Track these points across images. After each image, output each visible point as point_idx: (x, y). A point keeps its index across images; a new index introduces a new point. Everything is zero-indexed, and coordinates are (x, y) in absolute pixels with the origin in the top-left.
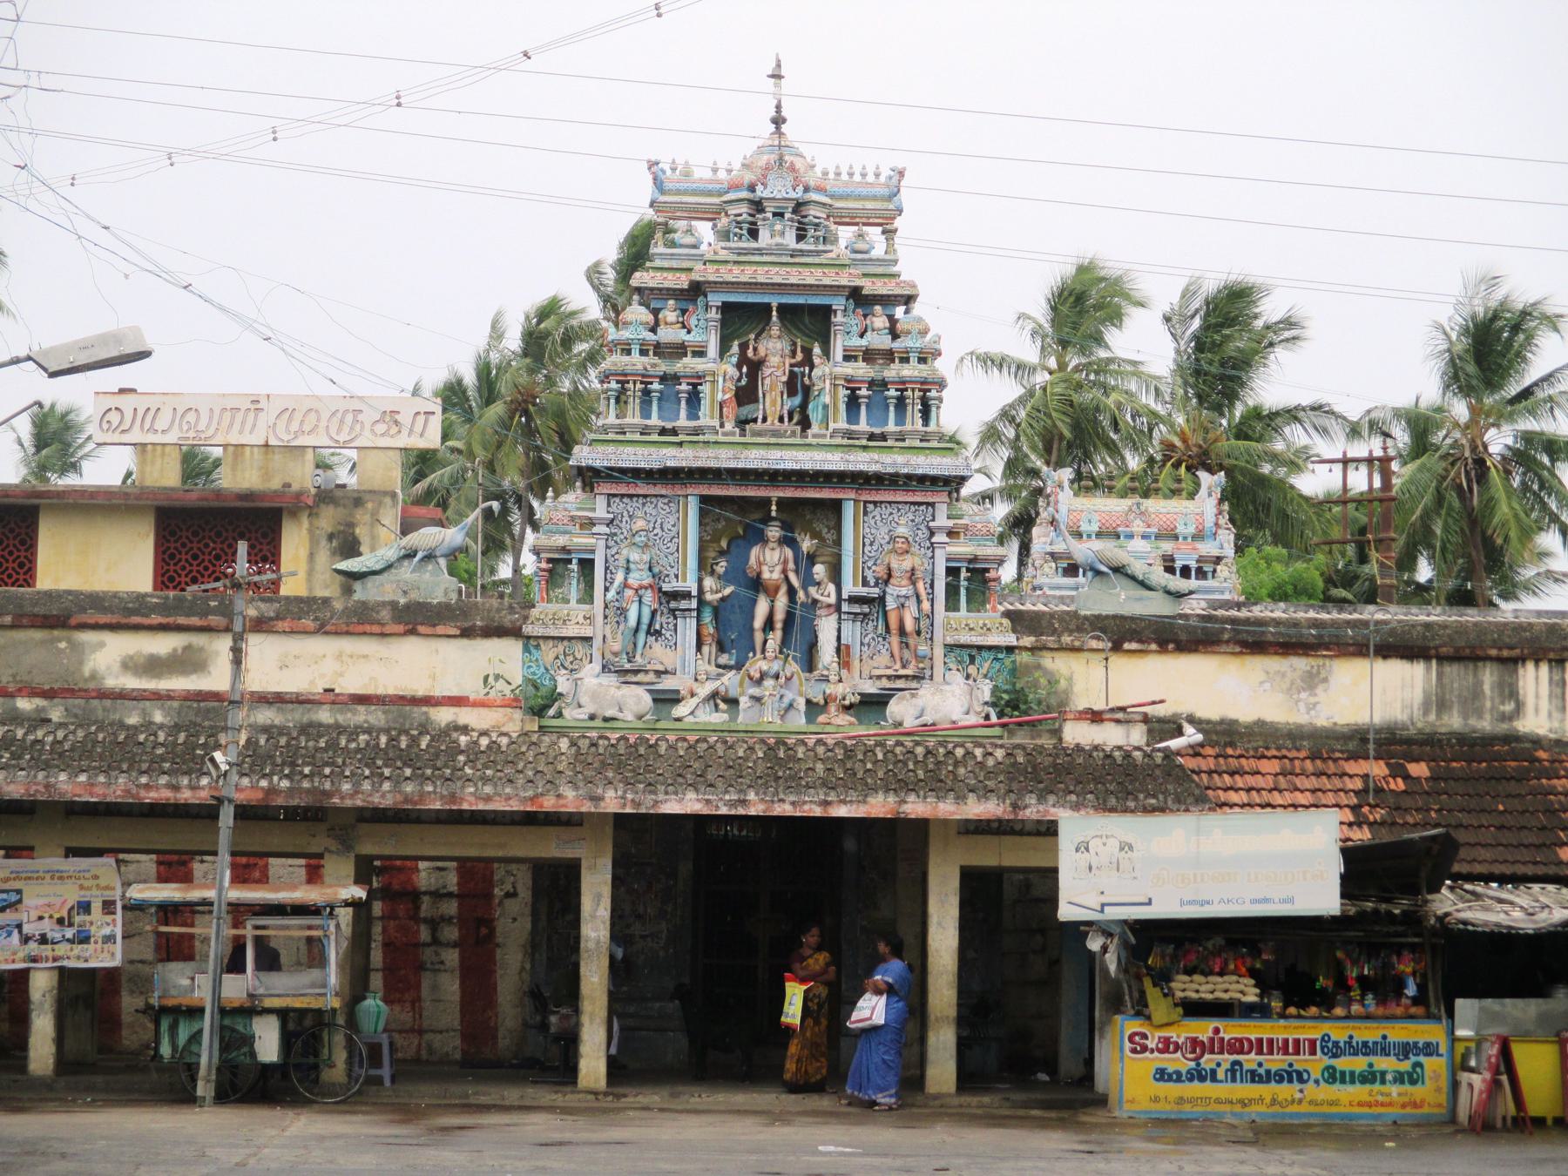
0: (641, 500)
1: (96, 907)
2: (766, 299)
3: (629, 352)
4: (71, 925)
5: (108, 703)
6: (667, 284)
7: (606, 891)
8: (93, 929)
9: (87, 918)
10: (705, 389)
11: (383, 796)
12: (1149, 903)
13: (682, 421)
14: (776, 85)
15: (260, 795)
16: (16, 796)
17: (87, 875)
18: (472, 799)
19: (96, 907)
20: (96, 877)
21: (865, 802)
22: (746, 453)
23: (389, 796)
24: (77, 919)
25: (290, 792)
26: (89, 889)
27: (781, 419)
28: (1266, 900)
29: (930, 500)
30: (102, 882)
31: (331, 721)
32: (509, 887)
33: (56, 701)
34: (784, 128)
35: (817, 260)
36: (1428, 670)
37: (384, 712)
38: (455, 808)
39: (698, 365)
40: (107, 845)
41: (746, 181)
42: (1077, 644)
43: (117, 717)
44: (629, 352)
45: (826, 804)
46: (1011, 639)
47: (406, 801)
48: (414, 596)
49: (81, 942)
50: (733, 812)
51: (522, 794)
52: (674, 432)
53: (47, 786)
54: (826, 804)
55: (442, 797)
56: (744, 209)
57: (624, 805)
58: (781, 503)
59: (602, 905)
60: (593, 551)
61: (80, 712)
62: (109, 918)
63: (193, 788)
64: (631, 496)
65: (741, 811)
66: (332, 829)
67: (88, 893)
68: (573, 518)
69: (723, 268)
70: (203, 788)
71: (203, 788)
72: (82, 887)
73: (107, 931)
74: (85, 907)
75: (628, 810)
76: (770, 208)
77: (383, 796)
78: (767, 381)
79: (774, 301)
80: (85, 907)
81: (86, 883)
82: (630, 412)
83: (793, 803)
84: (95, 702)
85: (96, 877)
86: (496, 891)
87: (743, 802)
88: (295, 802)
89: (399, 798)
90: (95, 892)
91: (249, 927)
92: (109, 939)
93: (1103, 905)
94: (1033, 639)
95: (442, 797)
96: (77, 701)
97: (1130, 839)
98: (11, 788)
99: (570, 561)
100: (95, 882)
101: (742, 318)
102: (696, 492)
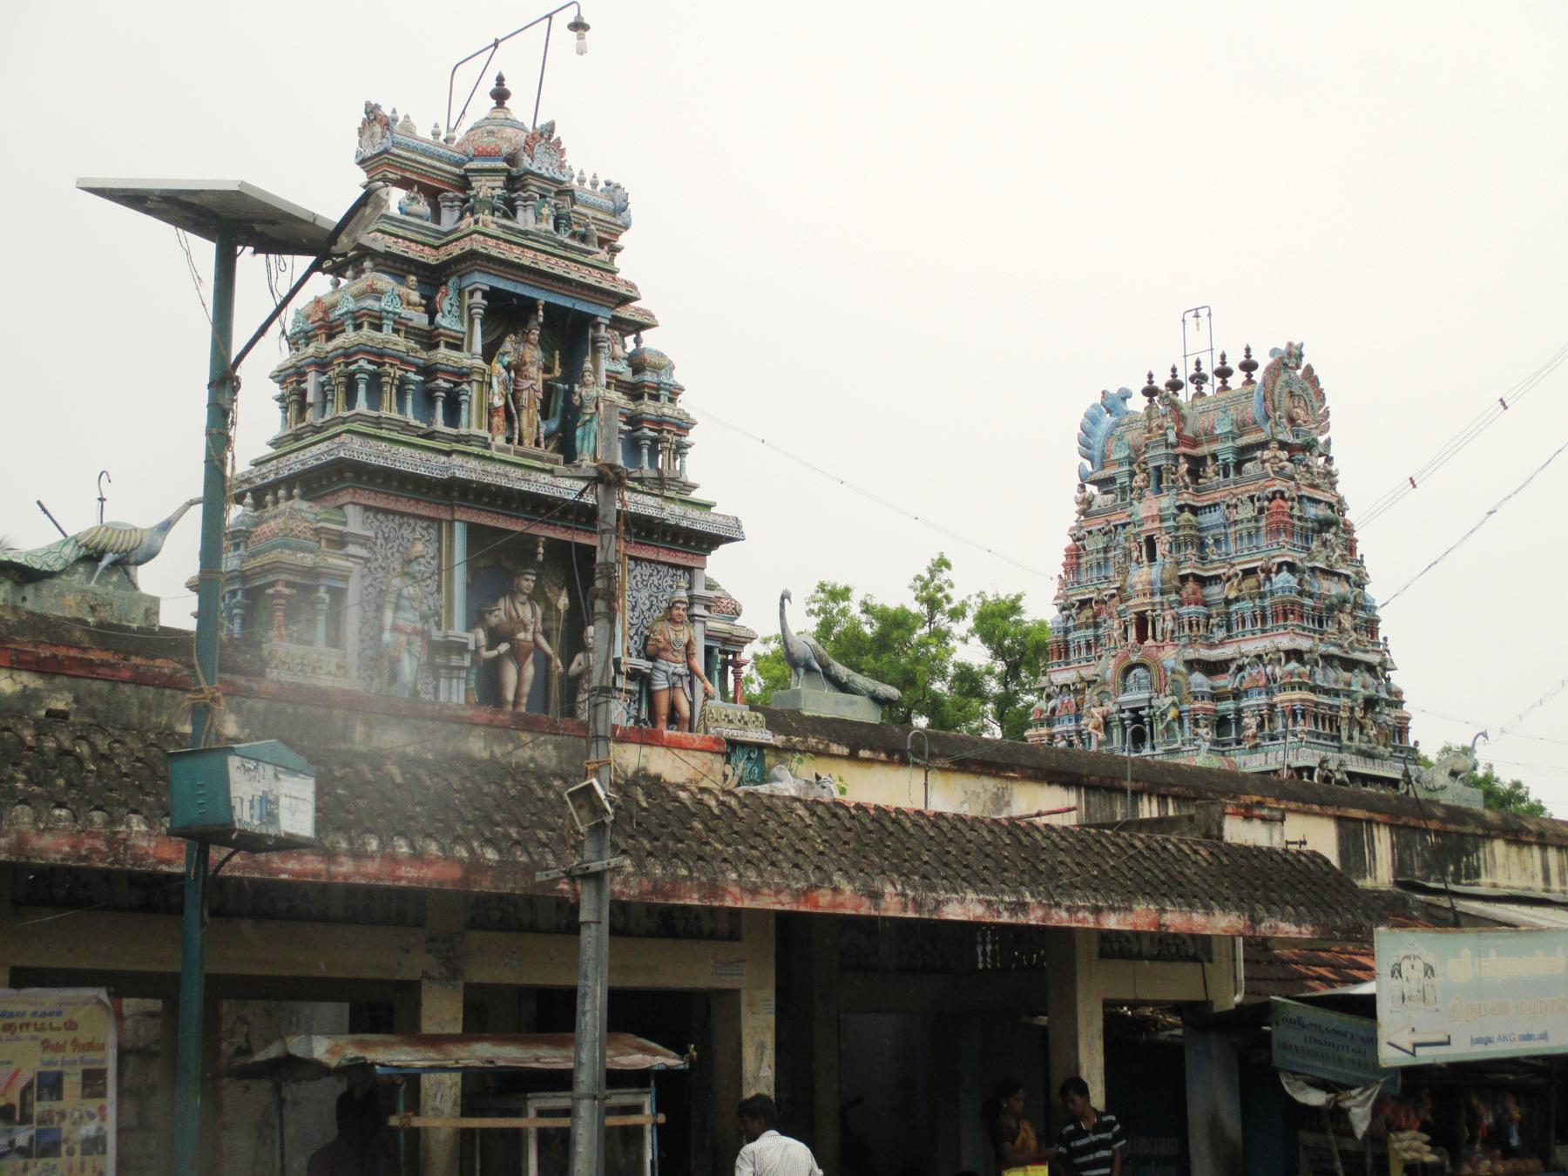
0: (397, 519)
1: (72, 1082)
2: (534, 294)
3: (379, 328)
4: (26, 1119)
5: (149, 693)
6: (411, 255)
7: (769, 1039)
8: (66, 1126)
9: (56, 1106)
10: (471, 391)
11: (625, 882)
12: (1448, 1043)
13: (440, 425)
14: (581, 38)
15: (458, 873)
16: (54, 858)
17: (58, 1022)
18: (736, 890)
19: (72, 1082)
20: (71, 1026)
21: (1130, 910)
22: (535, 475)
23: (633, 881)
24: (38, 1108)
25: (502, 868)
26: (59, 1048)
27: (537, 444)
28: (1528, 1037)
29: (679, 560)
30: (83, 1035)
31: (486, 755)
32: (240, 1041)
33: (58, 680)
34: (507, 103)
35: (581, 259)
36: (1079, 796)
37: (557, 747)
38: (716, 904)
39: (463, 359)
40: (85, 964)
41: (506, 149)
42: (821, 747)
43: (164, 719)
44: (379, 328)
45: (1097, 911)
46: (766, 737)
47: (656, 890)
48: (104, 614)
49: (44, 1153)
50: (1013, 921)
51: (795, 885)
52: (429, 435)
53: (112, 840)
54: (1022, 906)
55: (701, 885)
56: (499, 181)
57: (905, 908)
58: (552, 544)
59: (765, 1064)
60: (345, 578)
61: (100, 707)
62: (92, 1105)
63: (359, 855)
64: (386, 512)
65: (1021, 919)
66: (432, 940)
67: (58, 1057)
68: (317, 531)
69: (492, 242)
70: (371, 857)
71: (371, 857)
72: (46, 1045)
73: (89, 1129)
74: (51, 1084)
75: (911, 914)
76: (534, 187)
77: (625, 882)
78: (525, 395)
79: (542, 297)
80: (51, 1084)
81: (55, 1037)
82: (386, 404)
83: (1068, 909)
84: (127, 689)
85: (71, 1026)
86: (224, 1045)
87: (1022, 906)
88: (506, 888)
89: (647, 885)
90: (70, 1054)
91: (532, 1112)
92: (95, 1145)
93: (1416, 1045)
94: (783, 738)
95: (701, 885)
96: (96, 685)
97: (1431, 960)
98: (46, 841)
99: (316, 589)
100: (71, 1035)
101: (505, 314)
102: (464, 518)
